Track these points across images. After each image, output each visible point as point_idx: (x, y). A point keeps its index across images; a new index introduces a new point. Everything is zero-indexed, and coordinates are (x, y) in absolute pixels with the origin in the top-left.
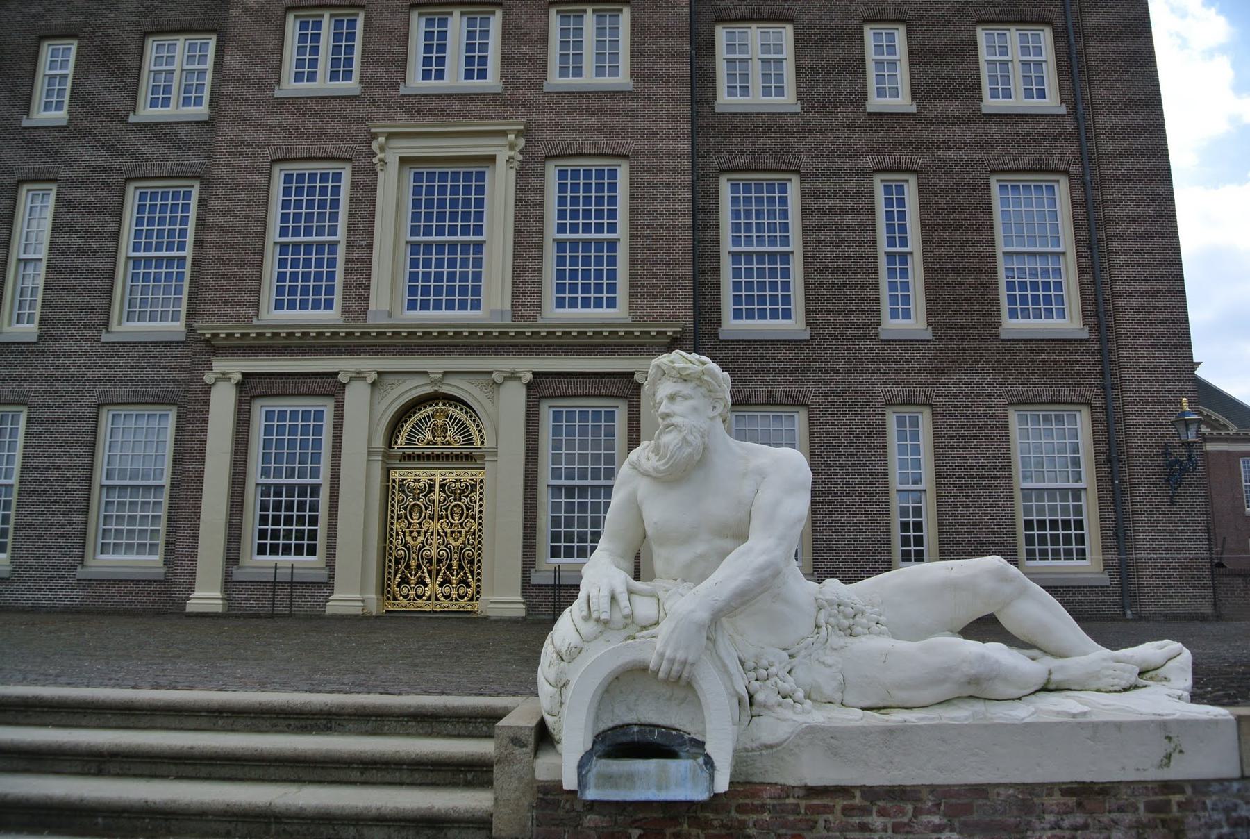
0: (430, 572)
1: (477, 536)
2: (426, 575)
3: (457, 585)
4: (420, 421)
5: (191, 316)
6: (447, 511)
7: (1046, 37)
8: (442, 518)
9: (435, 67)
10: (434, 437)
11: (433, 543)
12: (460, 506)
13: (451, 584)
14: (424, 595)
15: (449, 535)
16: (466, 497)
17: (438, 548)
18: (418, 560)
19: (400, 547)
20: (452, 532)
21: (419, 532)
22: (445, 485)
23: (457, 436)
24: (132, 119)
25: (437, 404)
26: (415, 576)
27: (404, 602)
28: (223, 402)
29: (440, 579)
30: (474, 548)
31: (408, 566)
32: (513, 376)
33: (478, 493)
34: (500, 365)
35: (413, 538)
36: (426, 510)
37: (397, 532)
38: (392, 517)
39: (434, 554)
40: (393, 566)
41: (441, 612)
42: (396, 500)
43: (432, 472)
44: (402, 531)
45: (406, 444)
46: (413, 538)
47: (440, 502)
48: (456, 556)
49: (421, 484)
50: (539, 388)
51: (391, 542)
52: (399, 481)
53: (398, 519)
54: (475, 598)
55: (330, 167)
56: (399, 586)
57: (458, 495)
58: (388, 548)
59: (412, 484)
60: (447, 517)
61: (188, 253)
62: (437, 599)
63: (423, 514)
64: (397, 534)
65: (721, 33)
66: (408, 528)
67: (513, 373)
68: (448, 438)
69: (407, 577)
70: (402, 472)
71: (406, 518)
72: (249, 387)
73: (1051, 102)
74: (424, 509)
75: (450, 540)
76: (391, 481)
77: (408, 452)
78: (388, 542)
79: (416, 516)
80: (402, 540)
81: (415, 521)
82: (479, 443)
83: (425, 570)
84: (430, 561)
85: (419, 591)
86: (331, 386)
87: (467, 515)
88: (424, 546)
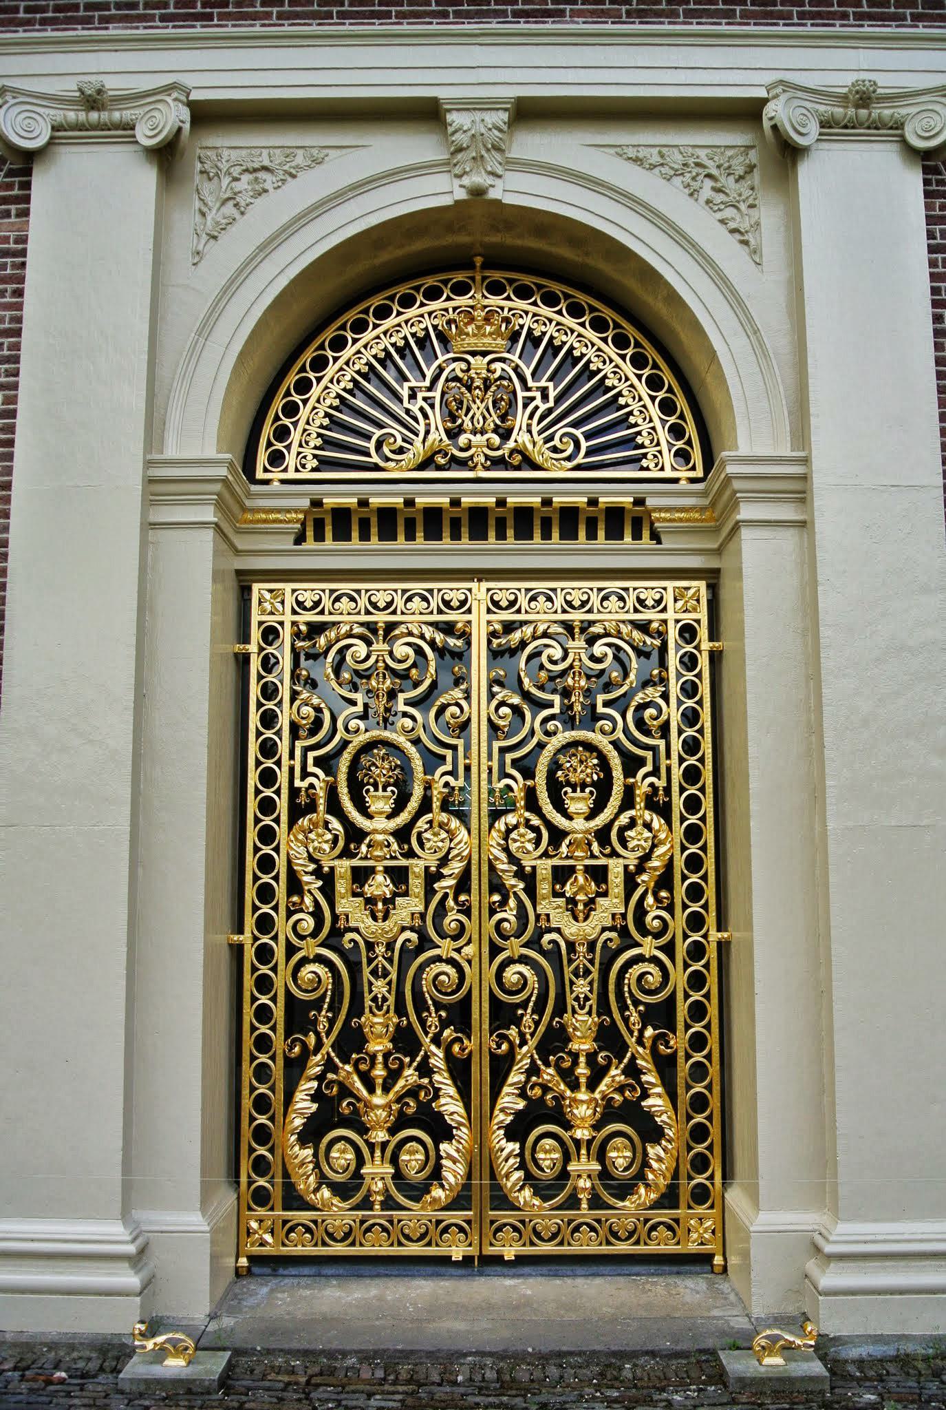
0: (460, 1070)
1: (680, 891)
2: (442, 1079)
3: (597, 1127)
4: (386, 360)
6: (528, 774)
8: (511, 808)
10: (453, 434)
11: (471, 926)
12: (590, 747)
13: (568, 1126)
14: (437, 1174)
15: (544, 888)
16: (619, 704)
17: (495, 950)
18: (400, 1010)
19: (311, 948)
20: (562, 875)
21: (399, 876)
22: (513, 652)
23: (561, 429)
25: (461, 289)
26: (386, 1089)
27: (339, 1213)
29: (510, 1101)
30: (669, 949)
31: (350, 1042)
33: (674, 689)
35: (370, 901)
36: (429, 770)
37: (292, 874)
38: (267, 806)
39: (481, 981)
40: (278, 1041)
41: (521, 1260)
42: (284, 722)
43: (454, 590)
44: (318, 873)
45: (324, 464)
46: (370, 901)
47: (493, 727)
48: (582, 987)
49: (401, 650)
51: (265, 924)
52: (297, 635)
53: (296, 812)
54: (685, 1195)
56: (312, 1133)
57: (577, 700)
58: (249, 954)
59: (361, 649)
60: (532, 803)
62: (502, 1200)
63: (418, 792)
64: (295, 886)
66: (346, 854)
67: (864, 98)
68: (520, 438)
69: (345, 1091)
70: (309, 592)
71: (334, 807)
74: (417, 764)
75: (552, 908)
76: (256, 634)
77: (346, 499)
78: (250, 922)
79: (380, 802)
80: (317, 914)
81: (381, 823)
82: (668, 459)
83: (438, 1059)
84: (459, 1015)
85: (412, 1159)
87: (629, 791)
88: (425, 942)
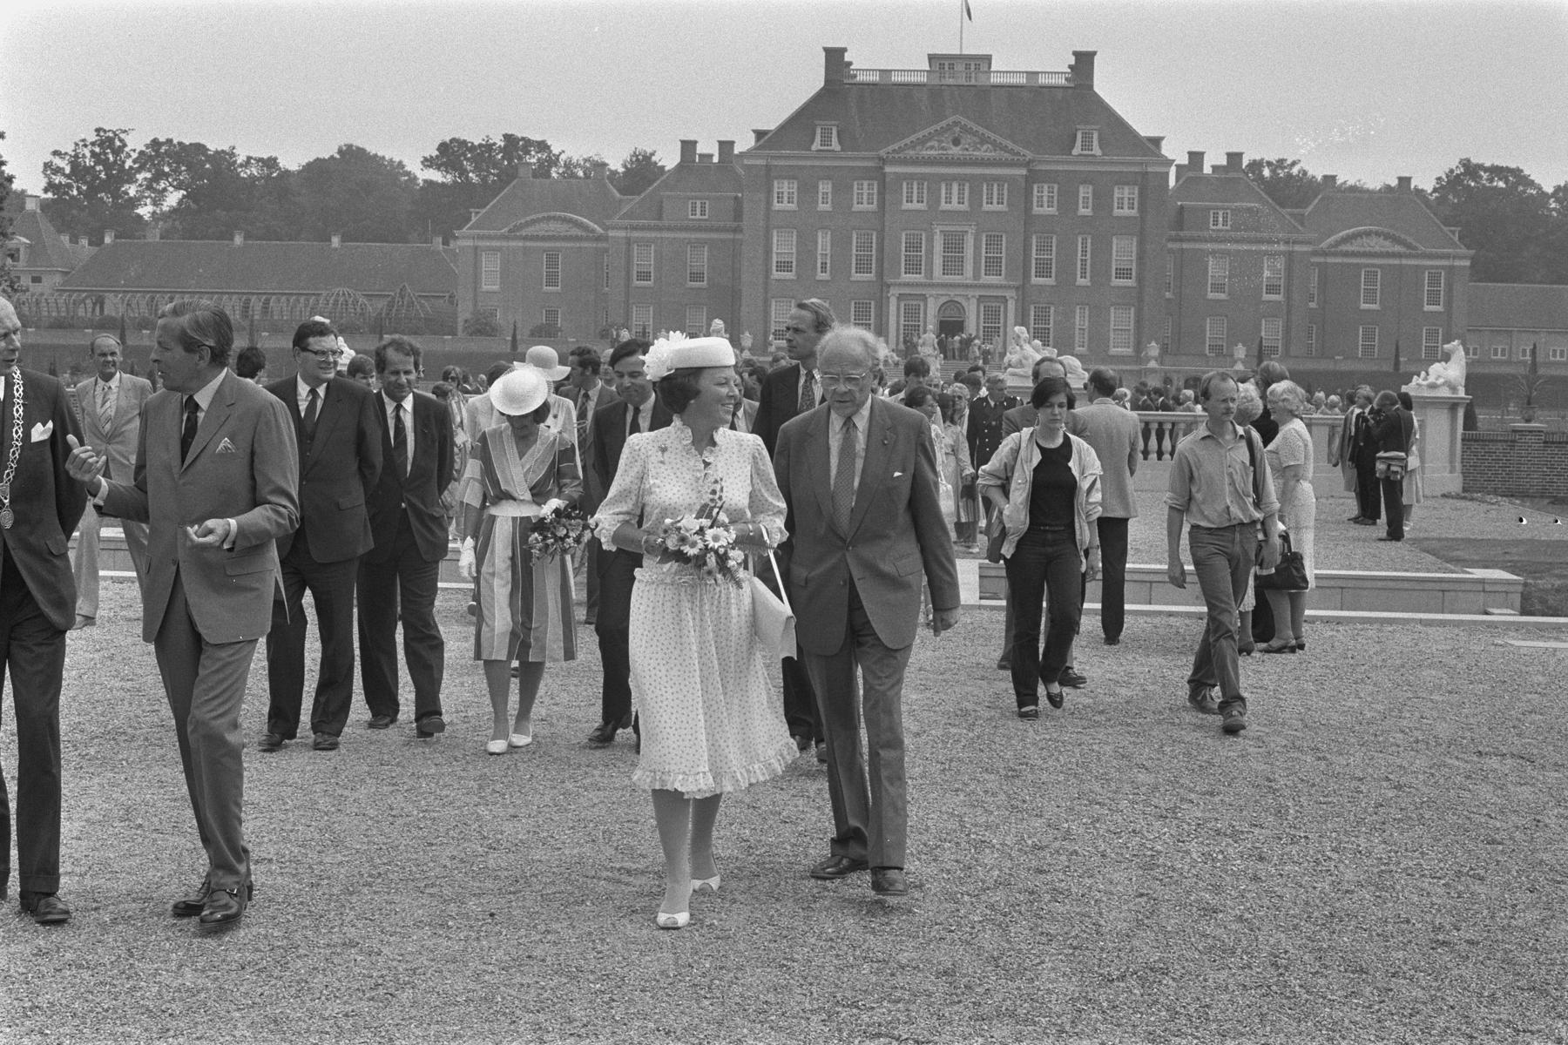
5: (880, 274)
7: (1136, 188)
9: (949, 201)
24: (853, 210)
28: (893, 302)
32: (973, 296)
34: (970, 293)
50: (980, 299)
55: (919, 232)
61: (874, 252)
65: (1035, 187)
72: (900, 297)
73: (1134, 212)
86: (924, 298)
